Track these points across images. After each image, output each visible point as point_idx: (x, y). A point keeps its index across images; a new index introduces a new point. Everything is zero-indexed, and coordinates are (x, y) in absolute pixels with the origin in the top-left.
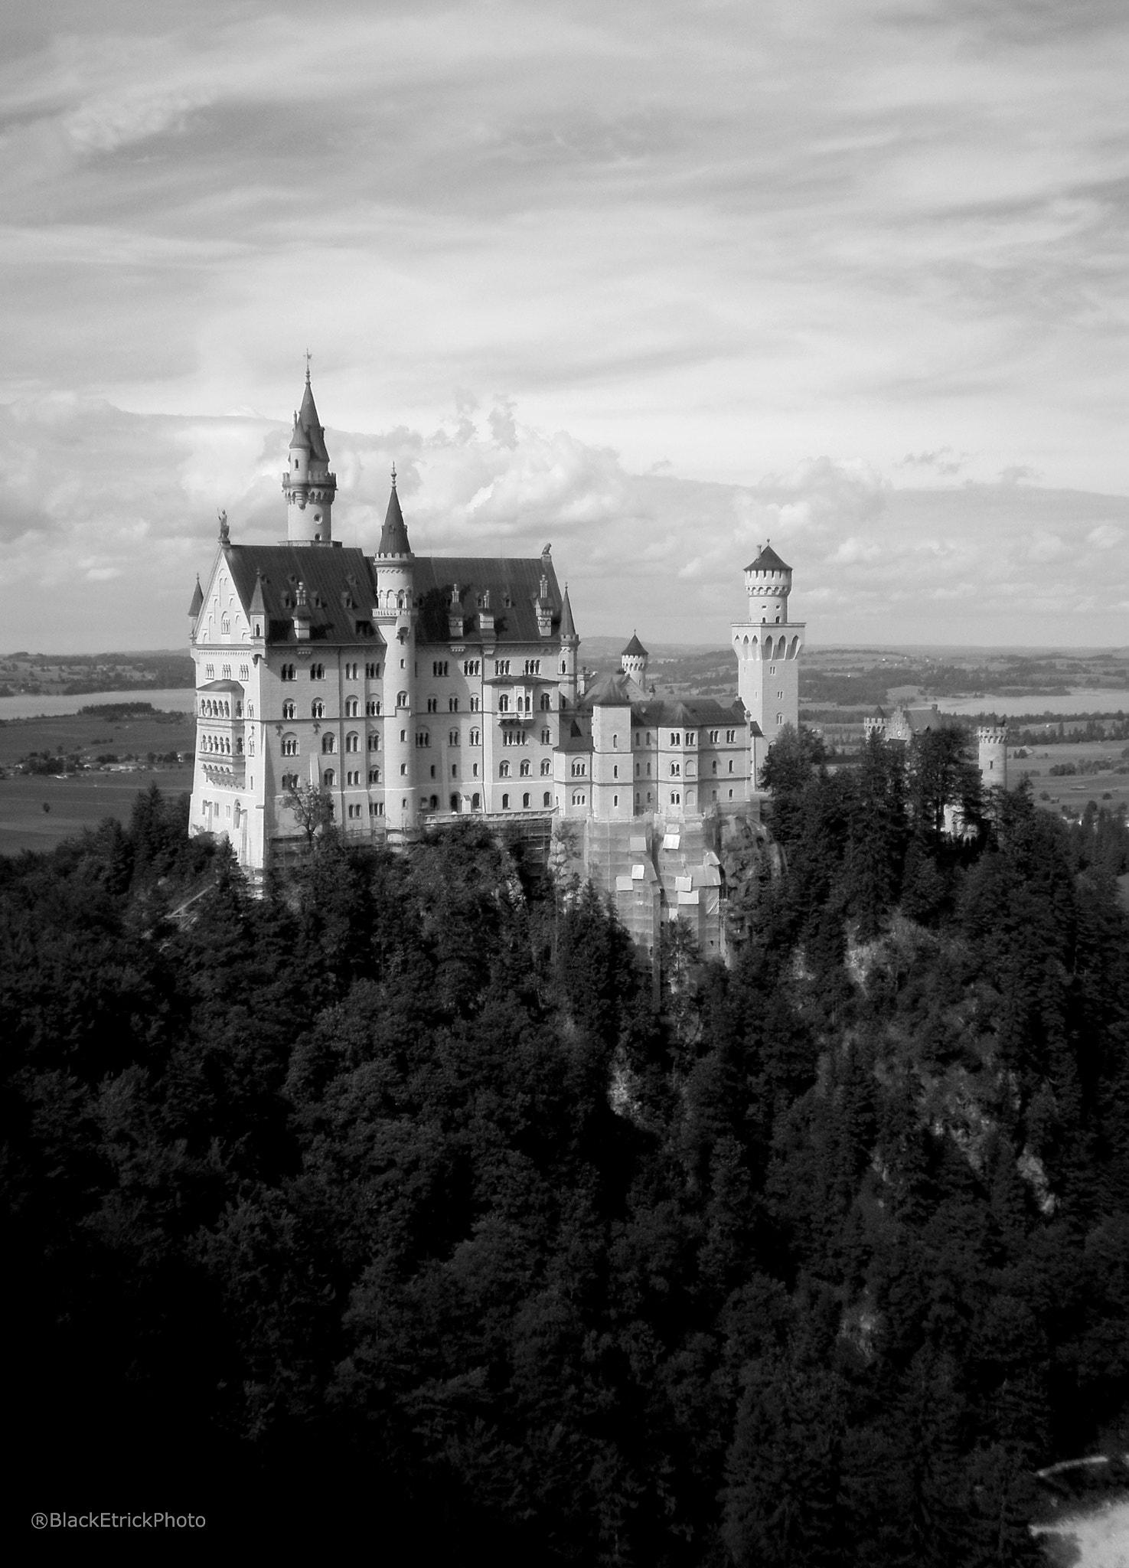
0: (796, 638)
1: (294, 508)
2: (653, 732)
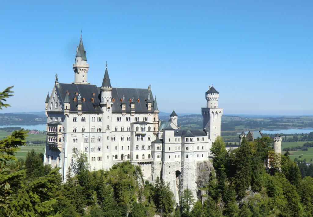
2: (180, 137)
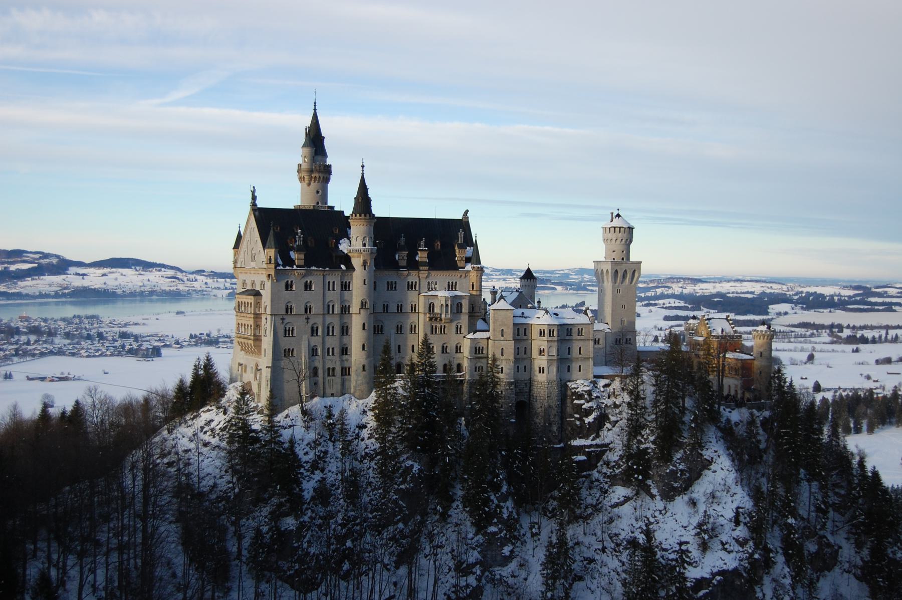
0: (635, 271)
1: (305, 184)
